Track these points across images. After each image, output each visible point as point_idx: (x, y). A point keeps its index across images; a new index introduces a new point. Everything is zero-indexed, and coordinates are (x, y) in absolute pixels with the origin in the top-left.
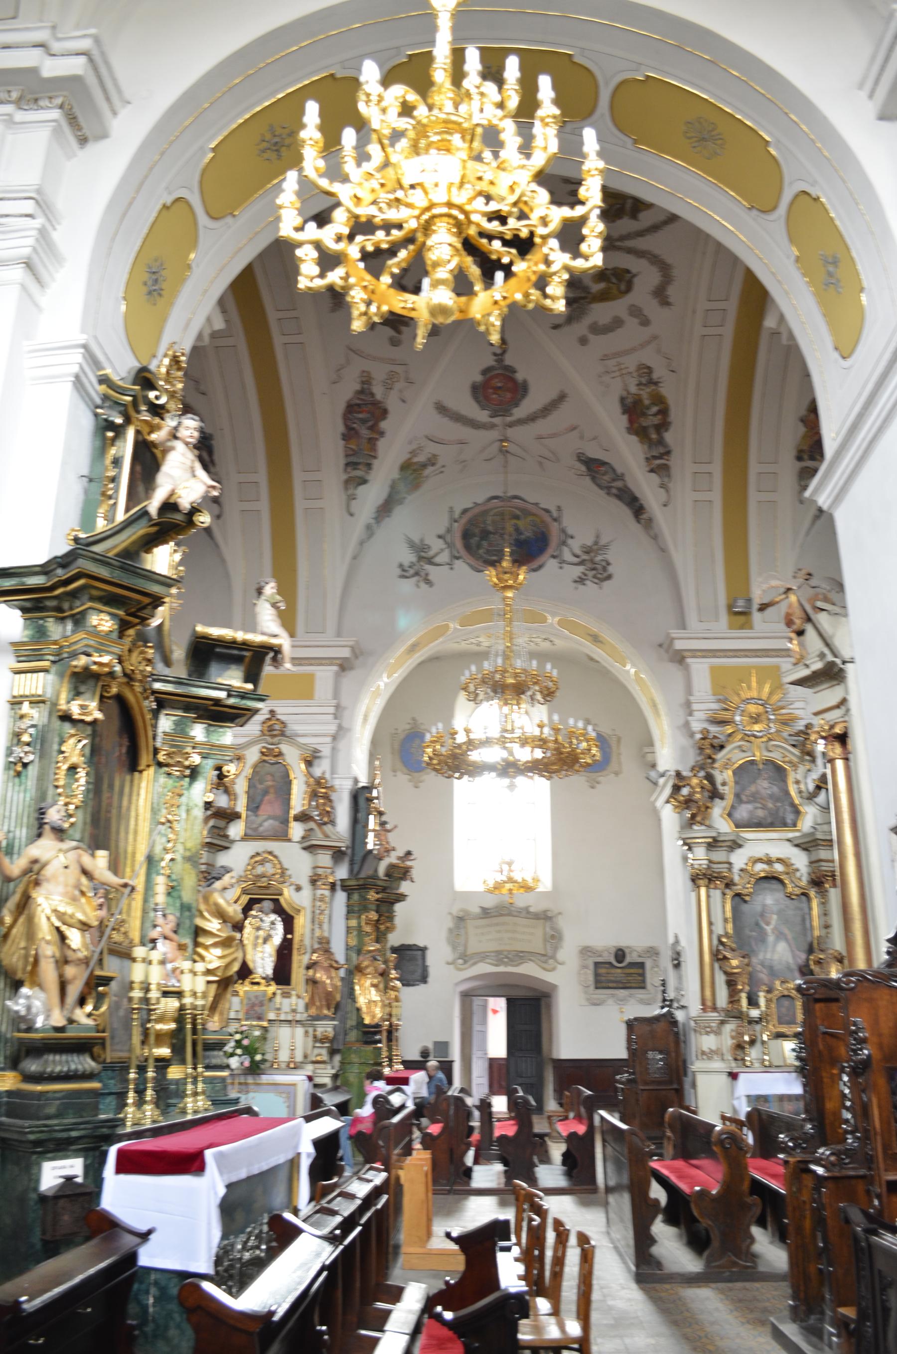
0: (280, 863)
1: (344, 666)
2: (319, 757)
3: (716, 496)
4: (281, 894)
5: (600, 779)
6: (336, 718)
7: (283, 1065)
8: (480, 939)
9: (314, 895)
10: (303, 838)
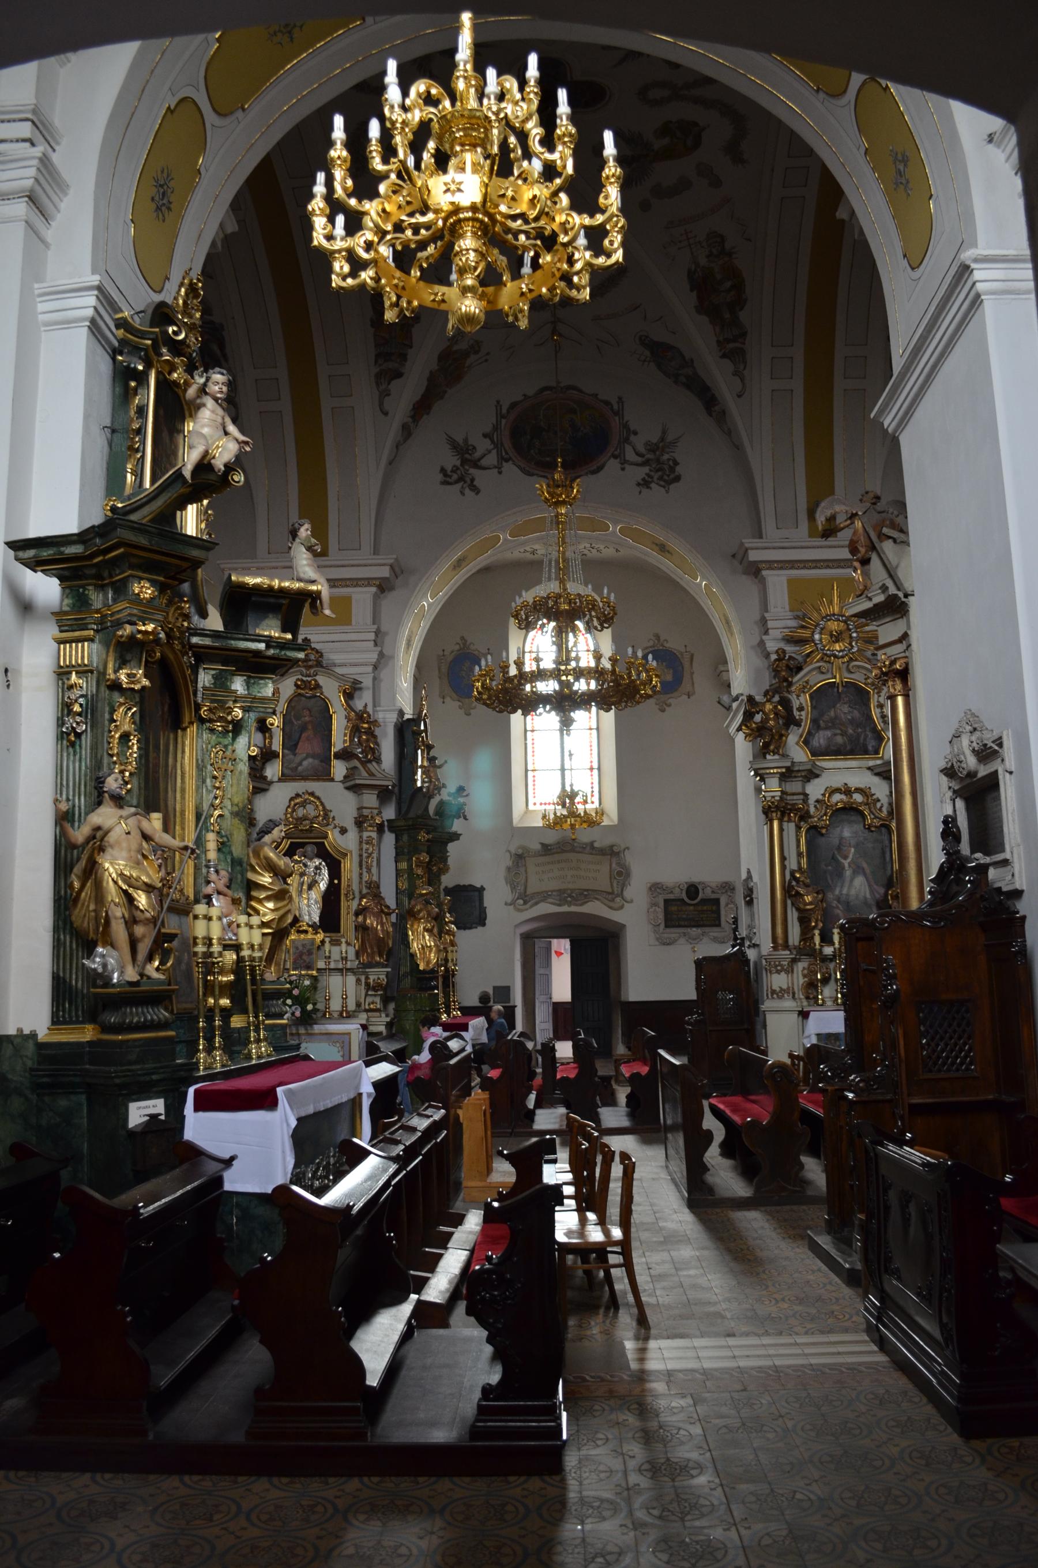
0: (322, 804)
1: (383, 587)
2: (360, 689)
3: (798, 385)
4: (326, 837)
5: (670, 701)
6: (376, 645)
7: (336, 1015)
8: (541, 877)
9: (361, 837)
10: (345, 777)
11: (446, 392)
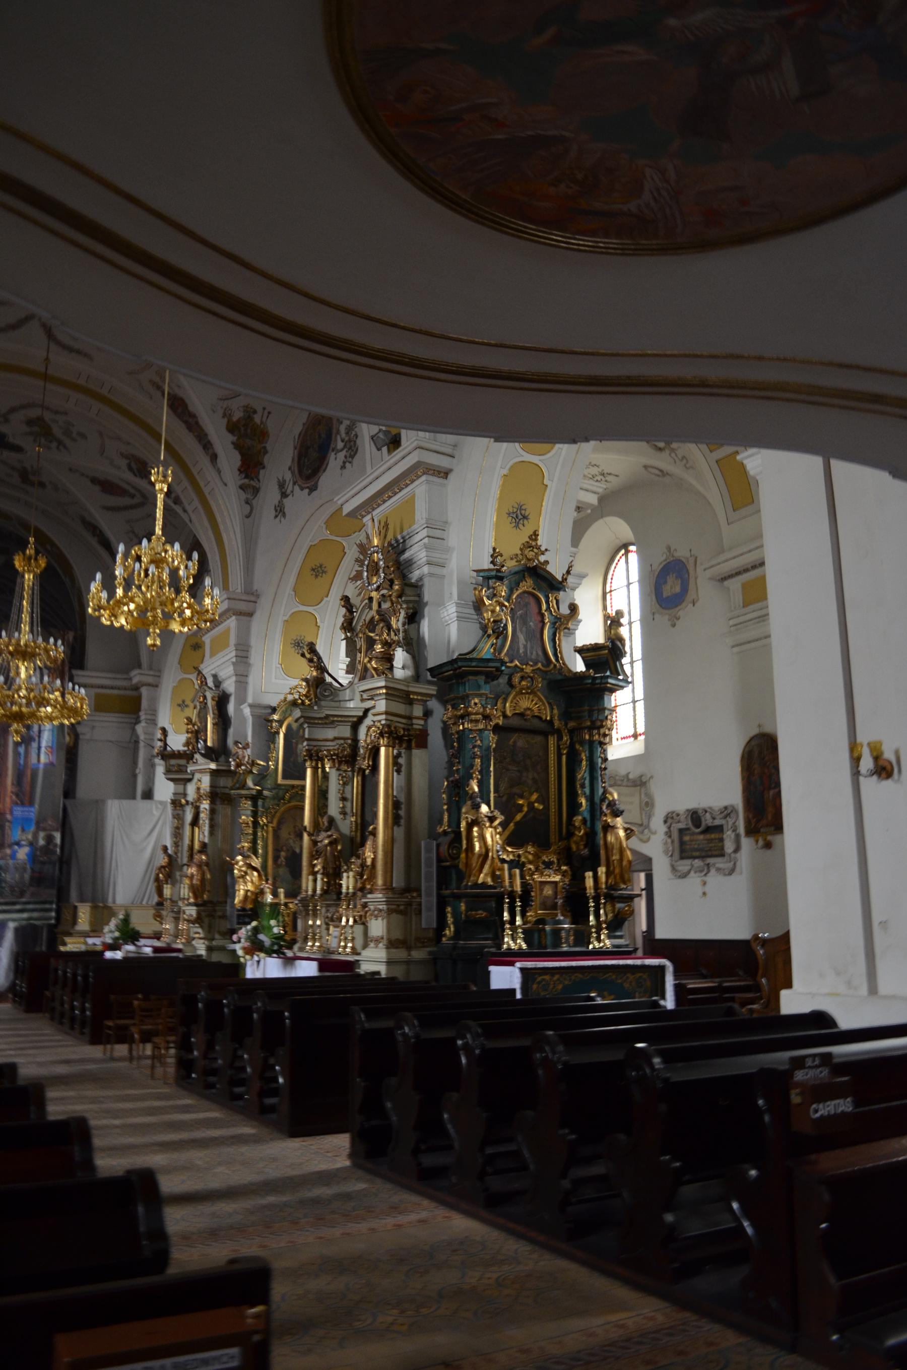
11: (265, 448)
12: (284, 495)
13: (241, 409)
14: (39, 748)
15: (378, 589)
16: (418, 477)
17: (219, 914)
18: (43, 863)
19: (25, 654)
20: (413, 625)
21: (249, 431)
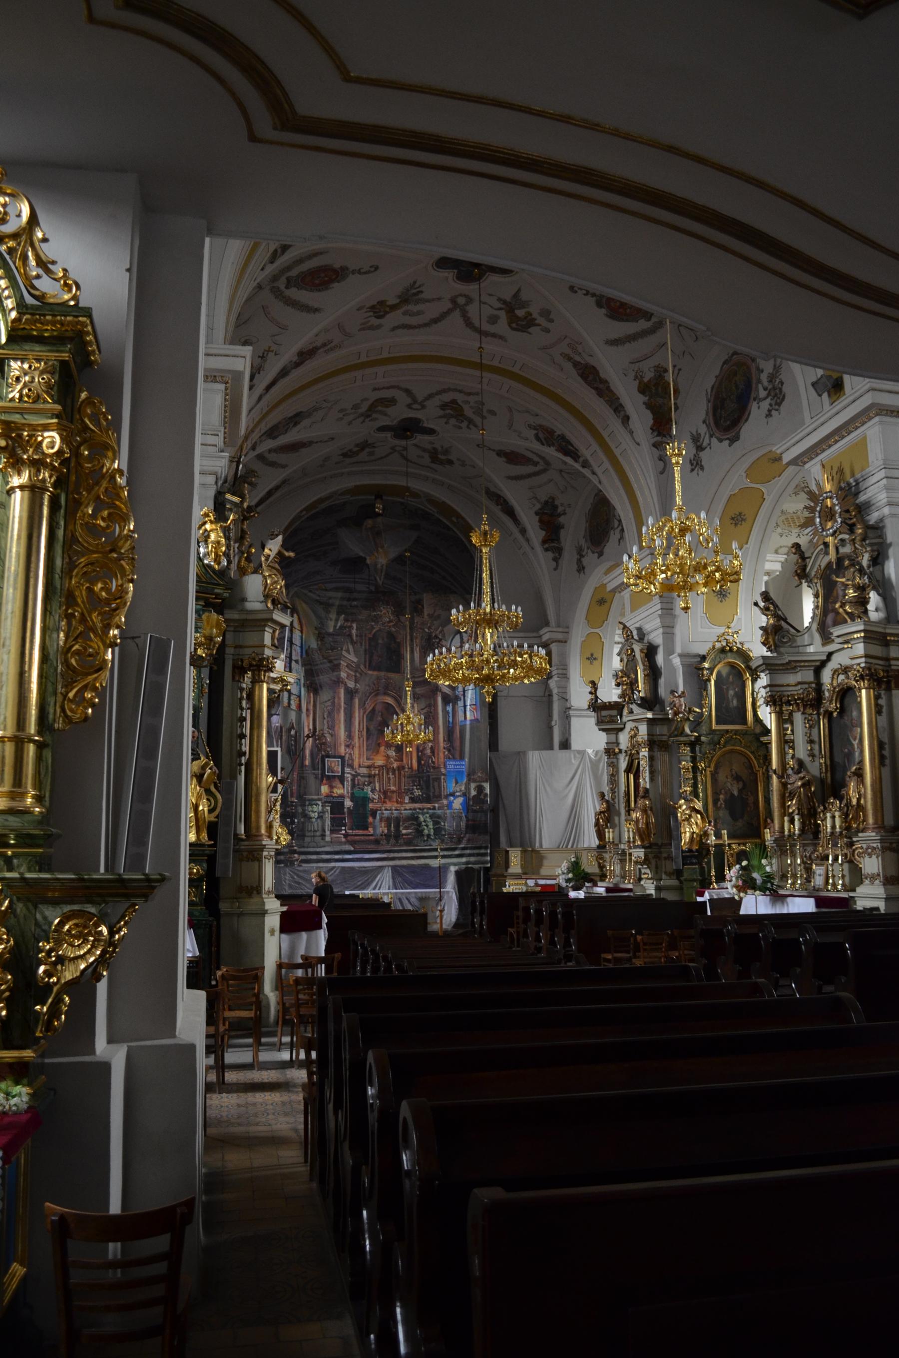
12: (700, 448)
13: (652, 370)
14: (465, 706)
15: (833, 534)
16: (870, 419)
17: (665, 855)
18: (475, 811)
19: (491, 622)
20: (877, 567)
21: (660, 389)
